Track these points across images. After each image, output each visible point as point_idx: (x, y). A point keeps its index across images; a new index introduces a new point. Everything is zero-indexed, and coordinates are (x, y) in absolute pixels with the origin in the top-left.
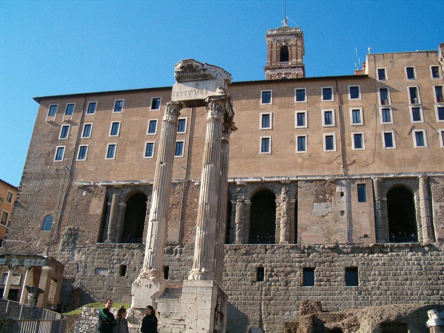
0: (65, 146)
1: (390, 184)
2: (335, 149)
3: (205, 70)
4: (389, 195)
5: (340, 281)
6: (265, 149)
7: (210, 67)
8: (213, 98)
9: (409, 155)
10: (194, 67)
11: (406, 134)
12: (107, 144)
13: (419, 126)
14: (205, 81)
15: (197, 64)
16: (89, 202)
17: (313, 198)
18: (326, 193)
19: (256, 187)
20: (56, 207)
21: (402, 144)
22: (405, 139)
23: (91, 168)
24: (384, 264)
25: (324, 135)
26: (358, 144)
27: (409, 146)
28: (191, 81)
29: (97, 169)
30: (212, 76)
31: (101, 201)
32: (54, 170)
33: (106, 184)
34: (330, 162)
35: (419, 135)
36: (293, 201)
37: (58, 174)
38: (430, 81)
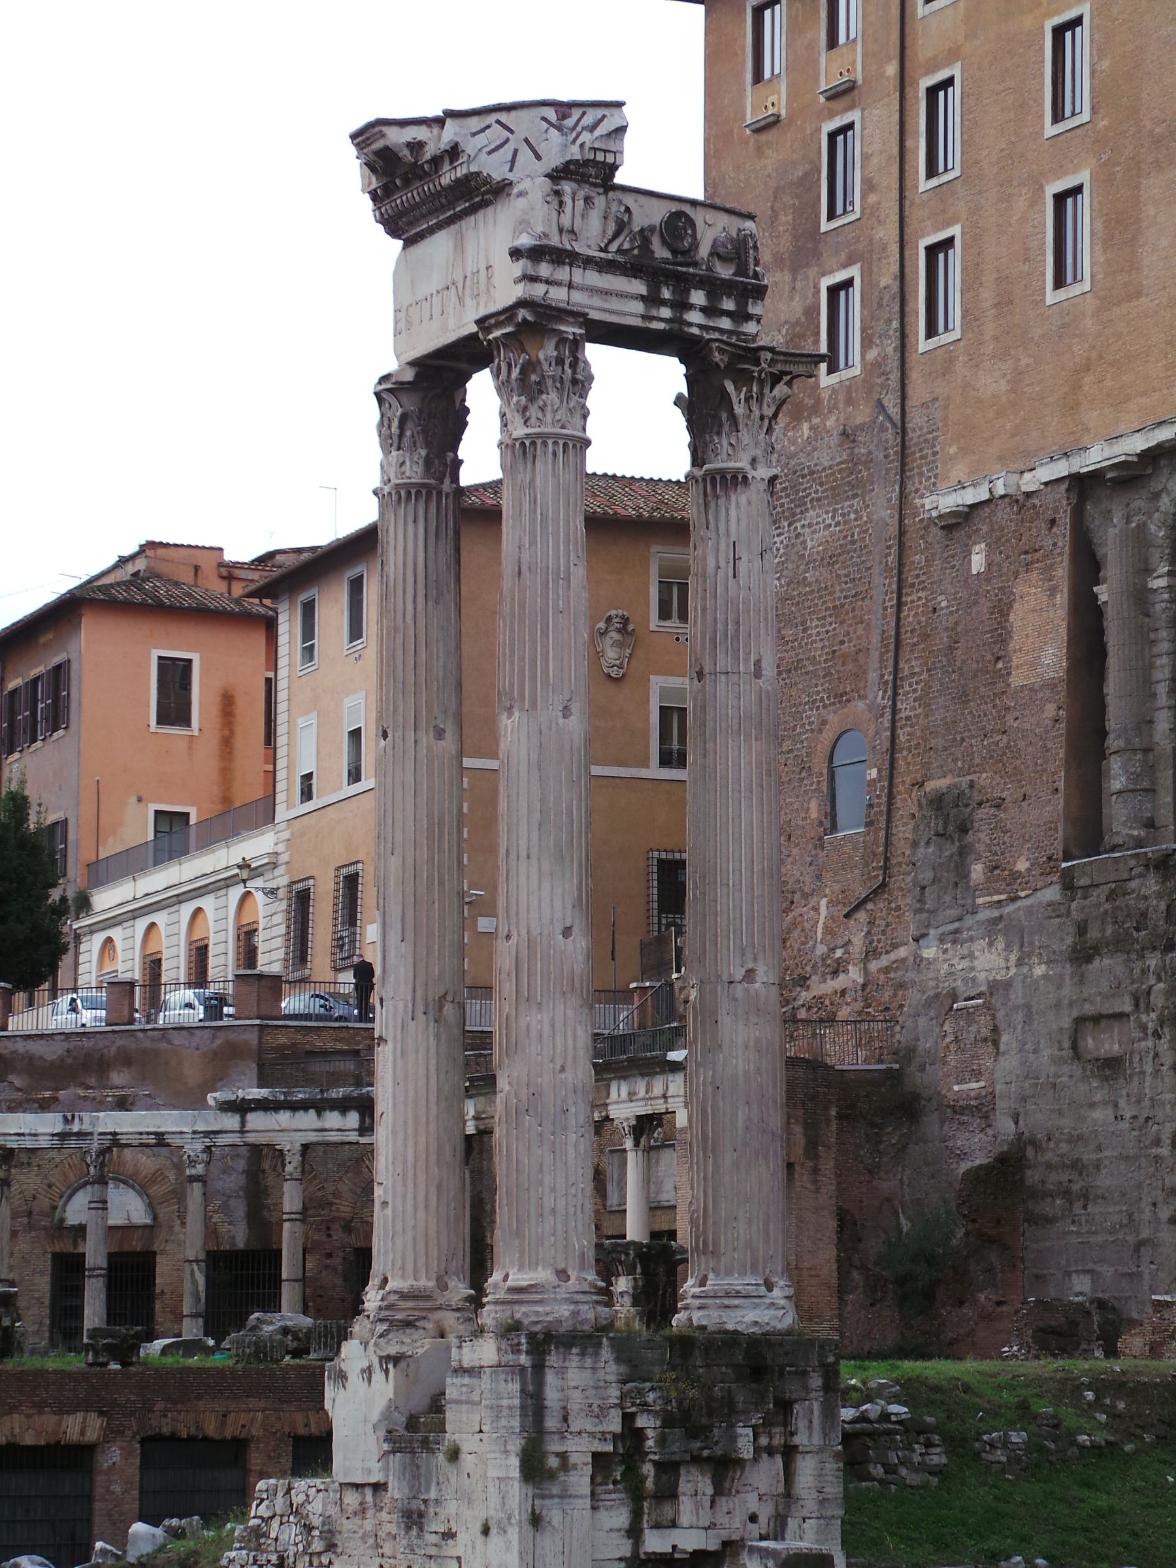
0: (854, 271)
3: (454, 152)
7: (474, 123)
8: (499, 325)
10: (406, 153)
12: (1041, 189)
14: (480, 215)
15: (411, 134)
16: (1003, 608)
20: (873, 676)
23: (991, 382)
28: (440, 226)
29: (1017, 379)
30: (487, 180)
31: (1053, 591)
32: (835, 439)
33: (1061, 469)
37: (854, 462)
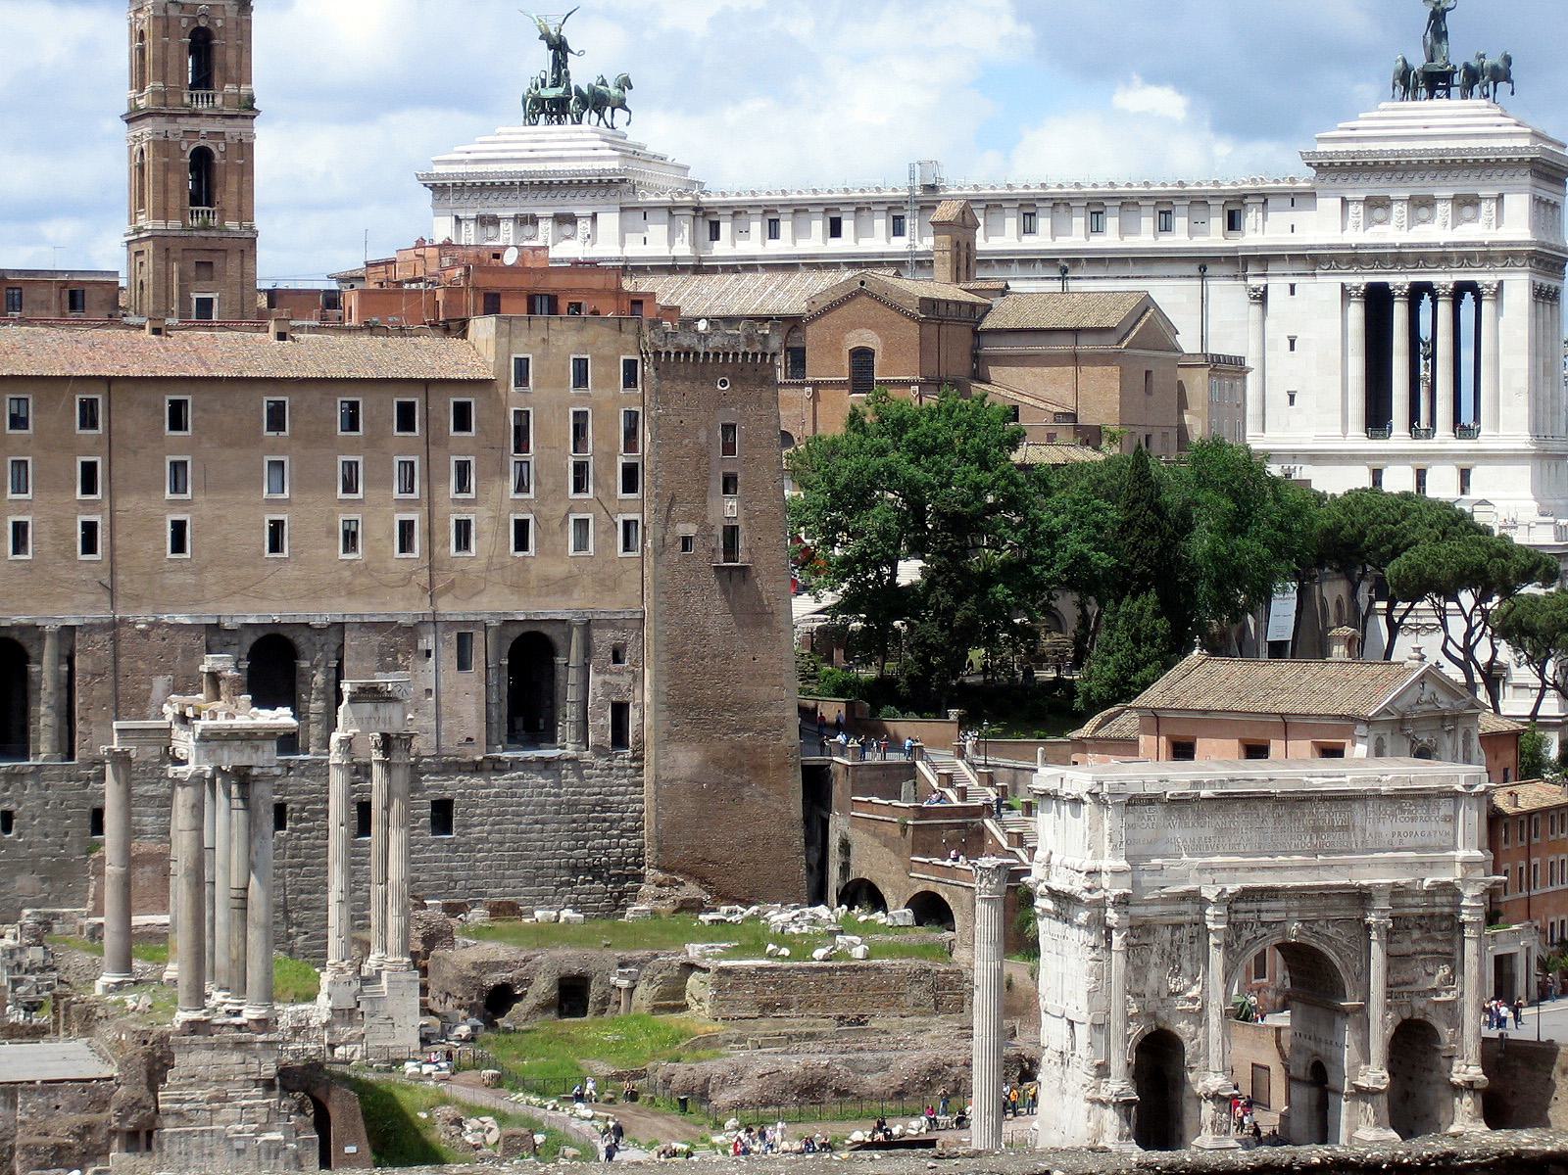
1: (517, 631)
2: (416, 554)
4: (511, 656)
5: (422, 827)
6: (276, 546)
9: (558, 570)
11: (556, 524)
13: (585, 506)
17: (375, 664)
18: (398, 652)
19: (261, 634)
21: (547, 544)
22: (553, 534)
24: (497, 795)
25: (398, 517)
26: (463, 542)
27: (558, 553)
34: (407, 581)
35: (581, 524)
36: (334, 664)
38: (616, 398)
